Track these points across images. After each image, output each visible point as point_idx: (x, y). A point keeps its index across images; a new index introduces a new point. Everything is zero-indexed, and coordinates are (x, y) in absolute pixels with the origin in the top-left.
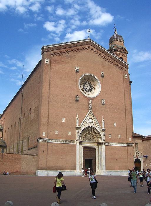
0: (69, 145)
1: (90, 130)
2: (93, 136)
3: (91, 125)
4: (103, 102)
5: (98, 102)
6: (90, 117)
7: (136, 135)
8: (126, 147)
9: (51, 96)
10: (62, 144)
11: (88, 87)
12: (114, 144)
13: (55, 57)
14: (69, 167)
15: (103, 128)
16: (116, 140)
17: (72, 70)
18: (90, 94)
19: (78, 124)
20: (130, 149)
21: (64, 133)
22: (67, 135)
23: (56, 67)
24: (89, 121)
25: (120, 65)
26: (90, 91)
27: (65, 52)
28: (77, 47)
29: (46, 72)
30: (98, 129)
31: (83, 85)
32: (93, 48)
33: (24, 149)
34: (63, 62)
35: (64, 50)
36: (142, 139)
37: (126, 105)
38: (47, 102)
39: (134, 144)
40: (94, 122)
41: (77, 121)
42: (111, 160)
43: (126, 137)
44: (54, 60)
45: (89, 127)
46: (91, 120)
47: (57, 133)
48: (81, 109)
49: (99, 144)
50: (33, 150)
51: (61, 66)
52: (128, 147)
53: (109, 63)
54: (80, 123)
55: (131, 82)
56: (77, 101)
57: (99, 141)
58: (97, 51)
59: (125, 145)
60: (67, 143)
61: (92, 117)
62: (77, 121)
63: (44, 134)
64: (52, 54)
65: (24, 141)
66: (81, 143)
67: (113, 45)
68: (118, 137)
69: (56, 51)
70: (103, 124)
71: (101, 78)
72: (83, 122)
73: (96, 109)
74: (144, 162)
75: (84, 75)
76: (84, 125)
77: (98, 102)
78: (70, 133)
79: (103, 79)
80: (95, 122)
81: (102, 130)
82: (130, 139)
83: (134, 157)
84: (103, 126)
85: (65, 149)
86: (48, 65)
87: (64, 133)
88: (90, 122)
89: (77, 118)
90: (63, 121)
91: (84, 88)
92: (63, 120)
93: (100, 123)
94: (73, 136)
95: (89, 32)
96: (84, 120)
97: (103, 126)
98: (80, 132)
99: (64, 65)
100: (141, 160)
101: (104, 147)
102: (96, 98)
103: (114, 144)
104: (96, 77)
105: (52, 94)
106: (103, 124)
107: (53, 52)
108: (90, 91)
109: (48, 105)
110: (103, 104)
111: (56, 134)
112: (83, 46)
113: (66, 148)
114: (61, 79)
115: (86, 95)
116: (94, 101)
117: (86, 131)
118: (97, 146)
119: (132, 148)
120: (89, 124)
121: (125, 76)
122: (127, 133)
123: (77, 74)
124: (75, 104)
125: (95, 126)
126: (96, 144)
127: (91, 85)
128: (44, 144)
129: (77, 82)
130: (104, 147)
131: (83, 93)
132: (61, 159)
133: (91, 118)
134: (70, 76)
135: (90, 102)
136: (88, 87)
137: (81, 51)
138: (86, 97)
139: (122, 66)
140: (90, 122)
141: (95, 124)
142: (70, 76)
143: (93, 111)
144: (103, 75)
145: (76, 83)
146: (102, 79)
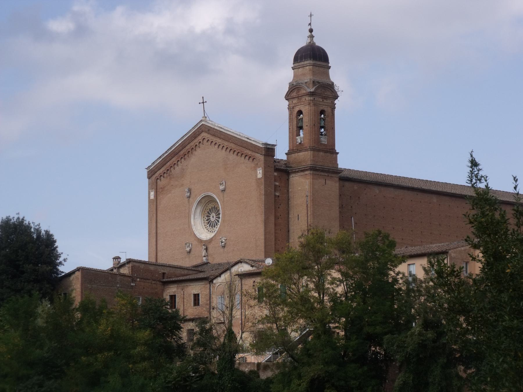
9: (159, 254)
25: (249, 153)
44: (161, 188)
51: (170, 195)
69: (161, 171)
102: (214, 239)
121: (258, 172)
124: (187, 259)
137: (194, 152)
139: (254, 154)
146: (223, 196)
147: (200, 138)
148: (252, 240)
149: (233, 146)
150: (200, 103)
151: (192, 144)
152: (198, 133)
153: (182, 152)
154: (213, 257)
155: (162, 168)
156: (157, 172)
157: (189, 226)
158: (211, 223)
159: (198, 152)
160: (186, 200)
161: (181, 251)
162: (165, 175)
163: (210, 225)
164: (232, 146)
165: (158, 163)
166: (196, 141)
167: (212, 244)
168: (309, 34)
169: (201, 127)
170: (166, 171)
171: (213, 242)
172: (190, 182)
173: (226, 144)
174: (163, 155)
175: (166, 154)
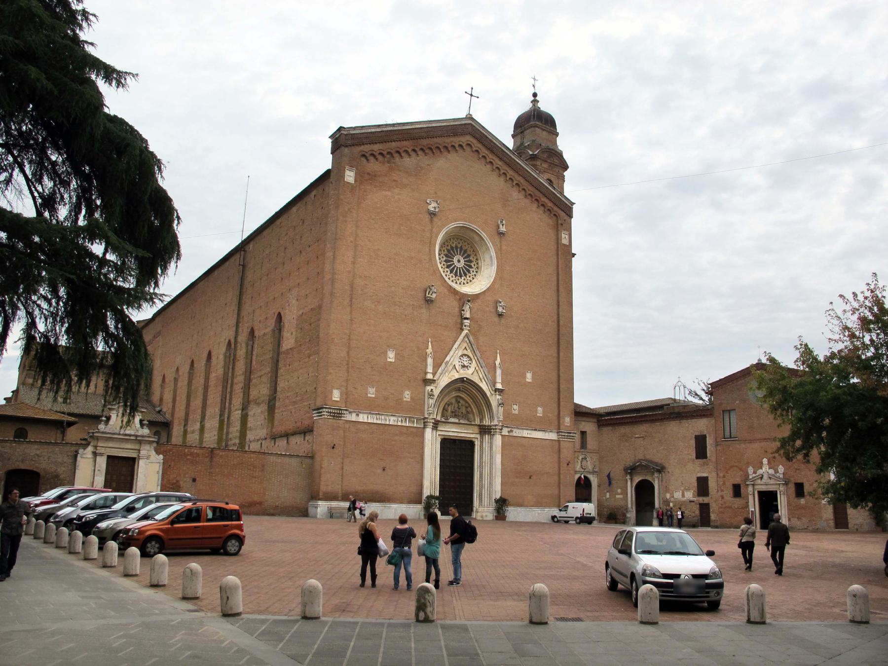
0: (405, 430)
1: (463, 385)
2: (470, 405)
3: (468, 373)
4: (500, 309)
5: (487, 309)
6: (465, 352)
7: (584, 410)
8: (557, 443)
10: (386, 428)
11: (459, 261)
12: (526, 433)
13: (373, 166)
14: (404, 493)
15: (499, 386)
16: (531, 421)
17: (418, 208)
18: (466, 283)
19: (430, 369)
20: (569, 446)
21: (392, 394)
22: (399, 401)
23: (376, 197)
24: (460, 363)
25: (550, 204)
26: (466, 275)
27: (401, 151)
28: (435, 140)
29: (346, 209)
30: (484, 386)
31: (446, 256)
32: (480, 146)
33: (250, 436)
34: (395, 181)
35: (398, 144)
36: (598, 421)
37: (561, 322)
38: (347, 301)
39: (578, 437)
40: (474, 364)
41: (430, 361)
42: (517, 477)
43: (556, 413)
44: (369, 174)
45: (461, 380)
46: (465, 359)
47: (372, 393)
48: (441, 325)
49: (485, 430)
50: (296, 440)
51: (389, 193)
52: (562, 442)
53: (521, 196)
54: (436, 366)
55: (574, 255)
56: (429, 301)
57: (486, 422)
58: (491, 157)
59: (553, 436)
60: (399, 424)
61: (469, 350)
62: (430, 361)
63: (336, 395)
64: (364, 156)
65: (251, 413)
66: (436, 426)
67: (525, 141)
68: (536, 411)
69: (376, 147)
70: (499, 372)
71: (497, 238)
72: (444, 364)
73: (480, 327)
74: (599, 486)
75: (452, 225)
76: (447, 374)
77: (487, 309)
78: (407, 396)
79: (504, 243)
80: (476, 365)
81: (496, 390)
82: (567, 420)
83: (576, 472)
84: (499, 379)
85: (393, 443)
86: (352, 187)
87: (392, 394)
88: (464, 366)
89: (429, 350)
90: (389, 360)
91: (449, 264)
92: (391, 356)
94: (417, 406)
95: (471, 95)
96: (448, 359)
97: (499, 379)
98: (436, 392)
99: (397, 191)
100: (594, 480)
101: (498, 440)
103: (526, 433)
104: (484, 235)
105: (360, 277)
107: (367, 148)
108: (466, 275)
109: (349, 309)
110: (500, 315)
111: (369, 395)
112: (452, 139)
113: (396, 438)
114: (386, 232)
115: (453, 285)
116: (476, 305)
117: (451, 391)
118: (478, 436)
119: (571, 445)
120: (462, 371)
121: (563, 235)
122: (562, 404)
123: (431, 221)
124: (424, 310)
125: (475, 379)
126: (476, 430)
127: (469, 256)
128: (335, 425)
129: (432, 245)
130: (498, 440)
131: (447, 279)
132: (380, 471)
133: (465, 355)
134: (413, 225)
135: (467, 308)
136: (459, 261)
137: (446, 153)
138: (455, 292)
139: (555, 208)
140: (464, 366)
141: (475, 373)
142: (413, 225)
143: (473, 335)
144: (503, 229)
145: (427, 250)
146: (500, 242)
148: (550, 322)
149: (522, 181)
150: (466, 92)
151: (448, 141)
152: (460, 131)
153: (425, 142)
154: (479, 325)
155: (378, 144)
156: (366, 146)
157: (430, 259)
158: (463, 270)
159: (454, 158)
160: (427, 217)
161: (412, 293)
162: (380, 158)
163: (451, 272)
164: (522, 181)
165: (371, 133)
166: (456, 140)
167: (476, 304)
168: (533, 98)
169: (467, 126)
170: (385, 153)
171: (479, 301)
172: (436, 193)
173: (511, 173)
174: (386, 125)
175: (391, 128)
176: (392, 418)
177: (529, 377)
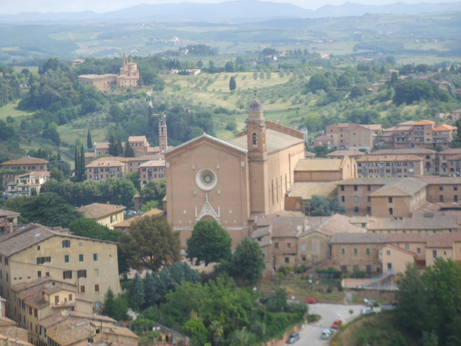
3: (209, 214)
13: (175, 160)
19: (196, 214)
25: (236, 154)
30: (214, 216)
41: (196, 212)
47: (180, 222)
56: (195, 195)
58: (212, 145)
69: (174, 154)
70: (219, 212)
82: (245, 224)
92: (185, 212)
93: (216, 211)
97: (219, 214)
106: (219, 212)
107: (171, 155)
125: (211, 215)
140: (207, 212)
147: (202, 142)
151: (197, 144)
153: (189, 148)
166: (200, 143)
173: (220, 148)
176: (186, 229)
177: (231, 212)
